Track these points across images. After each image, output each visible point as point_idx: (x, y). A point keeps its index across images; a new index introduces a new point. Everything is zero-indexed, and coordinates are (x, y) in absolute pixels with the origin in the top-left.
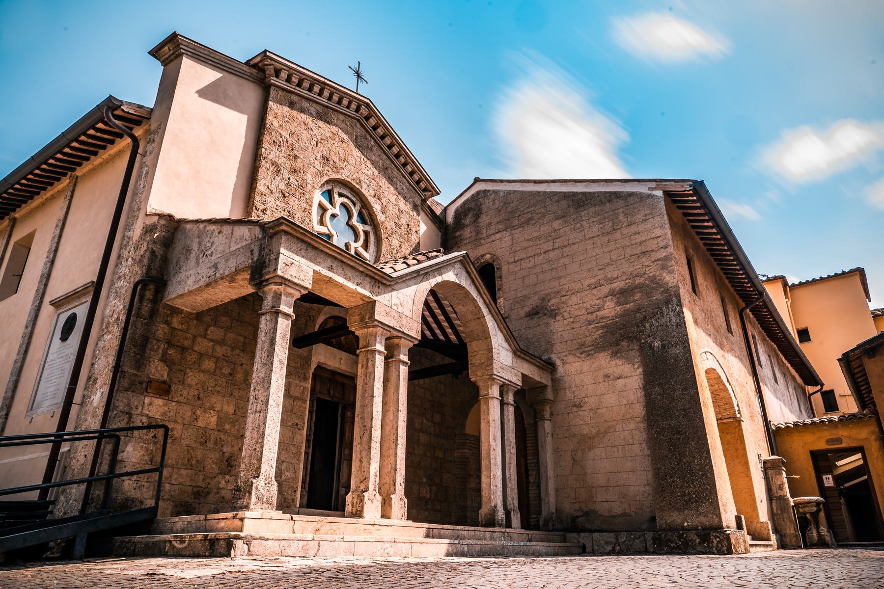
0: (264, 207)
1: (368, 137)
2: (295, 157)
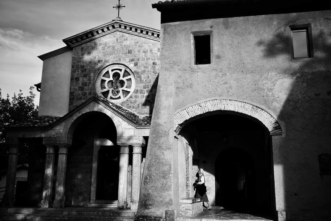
0: (73, 97)
1: (125, 34)
2: (85, 70)
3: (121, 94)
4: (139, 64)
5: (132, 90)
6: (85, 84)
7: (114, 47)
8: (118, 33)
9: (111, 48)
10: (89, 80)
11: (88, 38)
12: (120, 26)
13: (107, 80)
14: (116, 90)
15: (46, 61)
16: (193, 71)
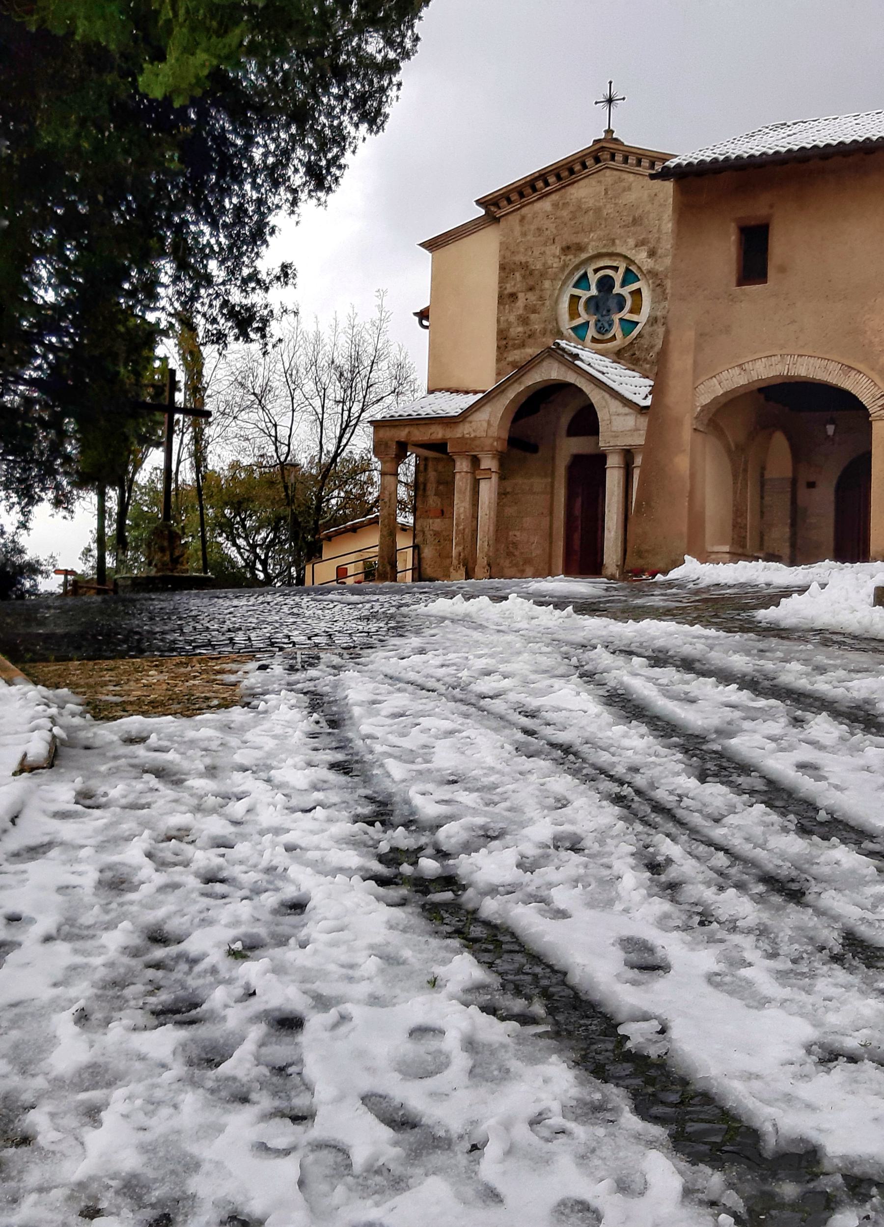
1: (625, 176)
3: (616, 330)
4: (660, 251)
5: (642, 318)
7: (598, 210)
8: (608, 172)
9: (591, 213)
10: (541, 298)
11: (534, 190)
12: (613, 158)
13: (584, 295)
14: (607, 318)
15: (439, 253)
16: (733, 299)
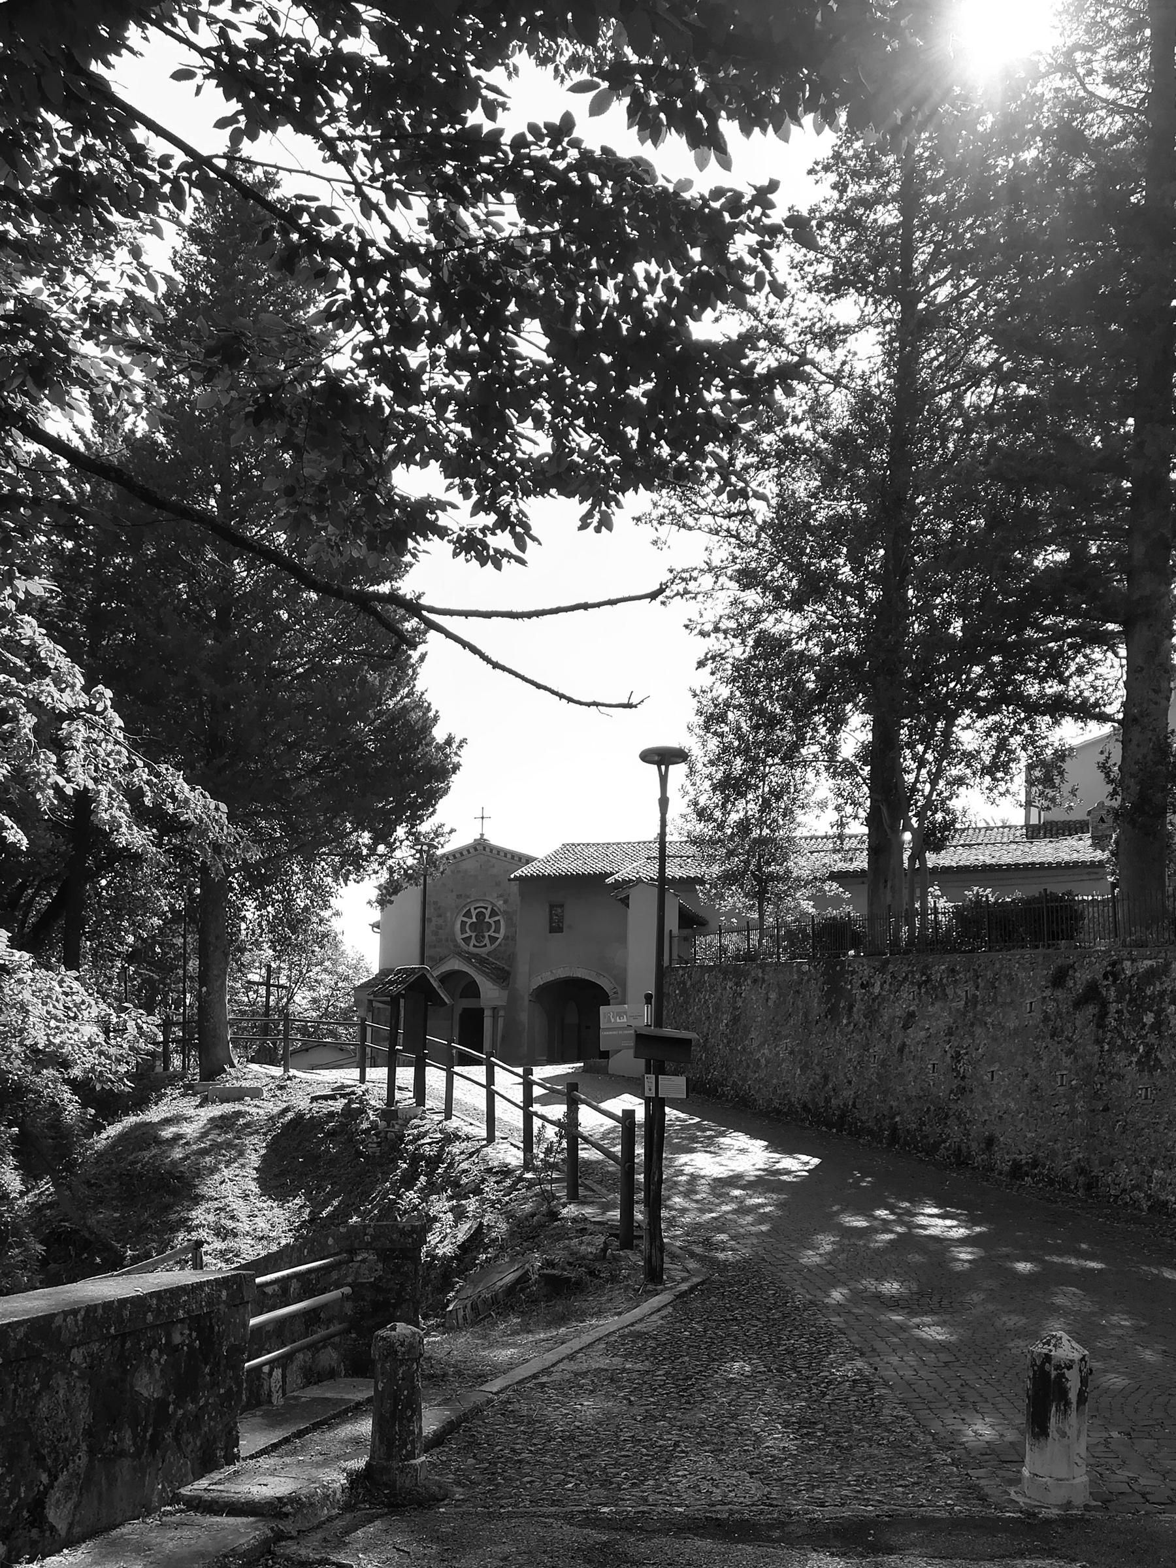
6: (439, 927)
13: (469, 921)
